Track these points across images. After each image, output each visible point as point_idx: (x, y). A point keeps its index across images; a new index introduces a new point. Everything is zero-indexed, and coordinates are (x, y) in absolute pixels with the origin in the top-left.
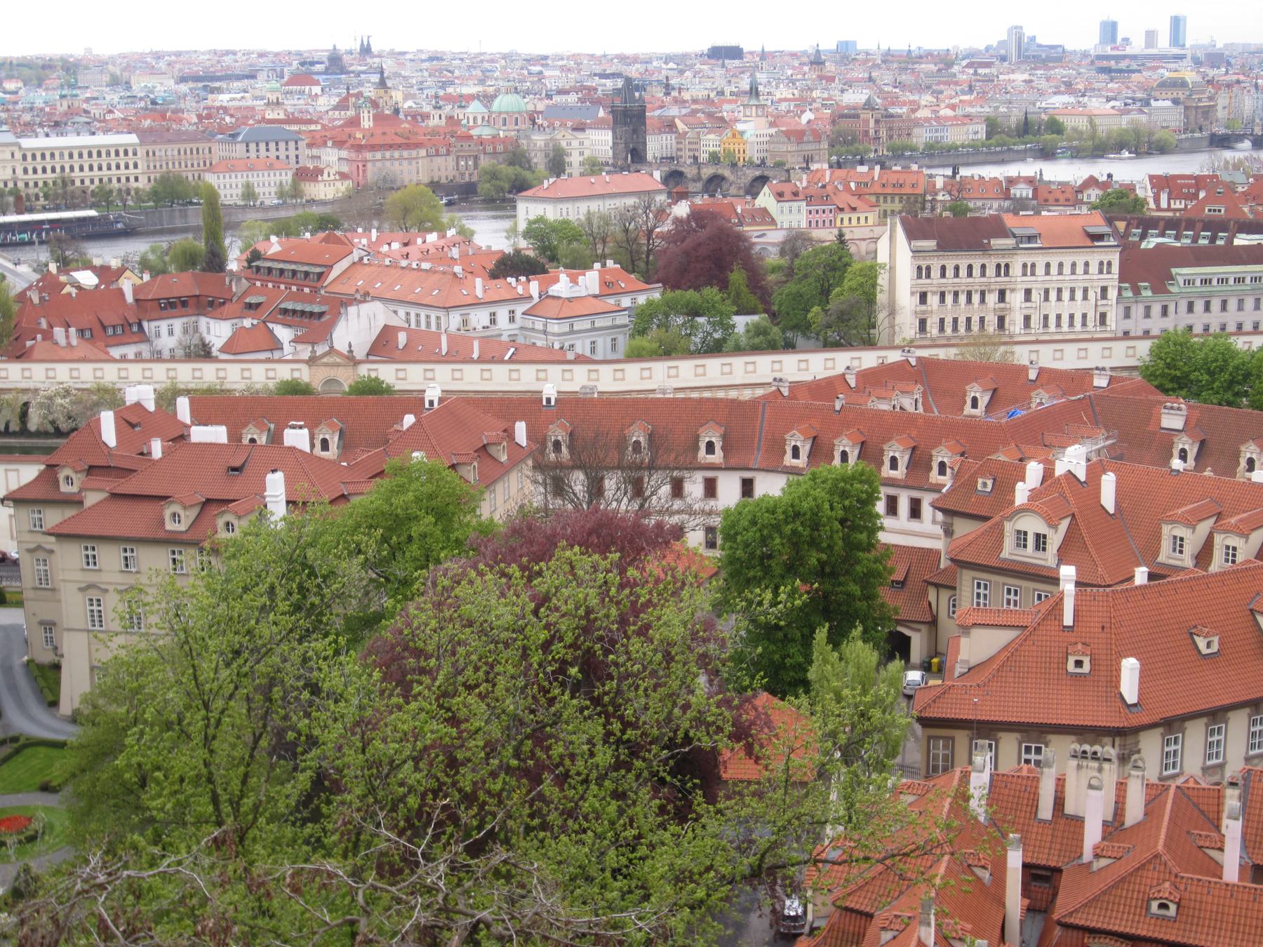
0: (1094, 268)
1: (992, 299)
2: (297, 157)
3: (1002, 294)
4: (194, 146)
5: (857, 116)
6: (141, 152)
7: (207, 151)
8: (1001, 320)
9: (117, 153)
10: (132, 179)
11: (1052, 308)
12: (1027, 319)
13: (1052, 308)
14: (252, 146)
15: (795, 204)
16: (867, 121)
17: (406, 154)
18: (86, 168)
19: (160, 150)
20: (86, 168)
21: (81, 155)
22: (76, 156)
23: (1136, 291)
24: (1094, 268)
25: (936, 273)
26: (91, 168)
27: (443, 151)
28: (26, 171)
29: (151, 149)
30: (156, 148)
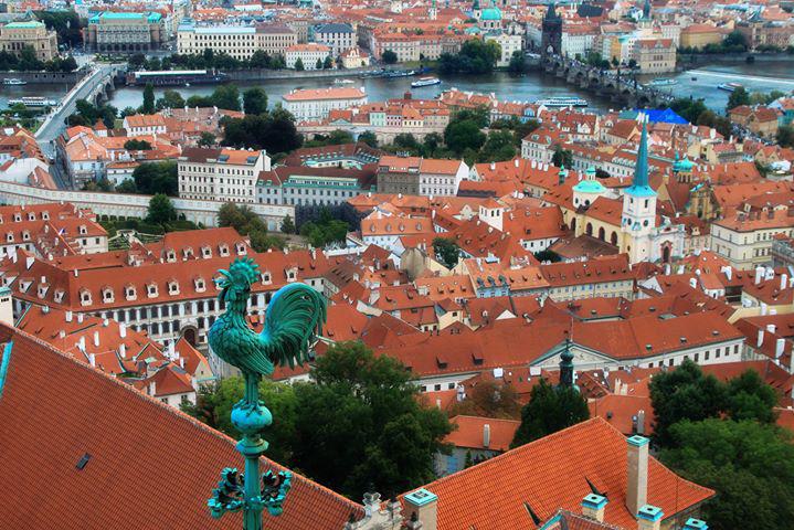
0: (246, 173)
1: (208, 180)
3: (212, 180)
5: (747, 25)
6: (256, 37)
8: (212, 189)
11: (231, 186)
12: (222, 189)
13: (231, 186)
14: (325, 35)
15: (380, 114)
16: (751, 29)
17: (404, 44)
23: (265, 183)
24: (246, 173)
25: (187, 169)
28: (197, 45)
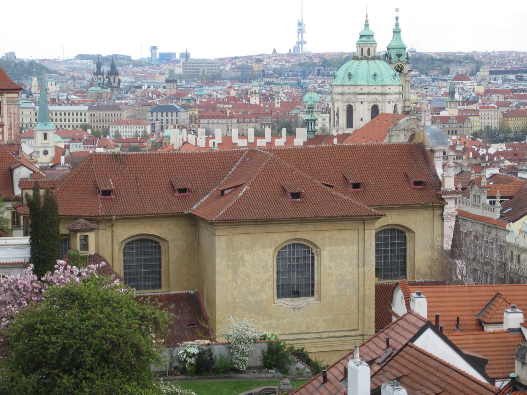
2: (177, 120)
4: (113, 113)
6: (88, 114)
7: (119, 115)
9: (77, 114)
10: (67, 126)
14: (155, 114)
18: (63, 120)
19: (97, 113)
20: (63, 120)
21: (61, 114)
22: (58, 115)
26: (65, 120)
27: (253, 120)
29: (93, 113)
30: (95, 112)
